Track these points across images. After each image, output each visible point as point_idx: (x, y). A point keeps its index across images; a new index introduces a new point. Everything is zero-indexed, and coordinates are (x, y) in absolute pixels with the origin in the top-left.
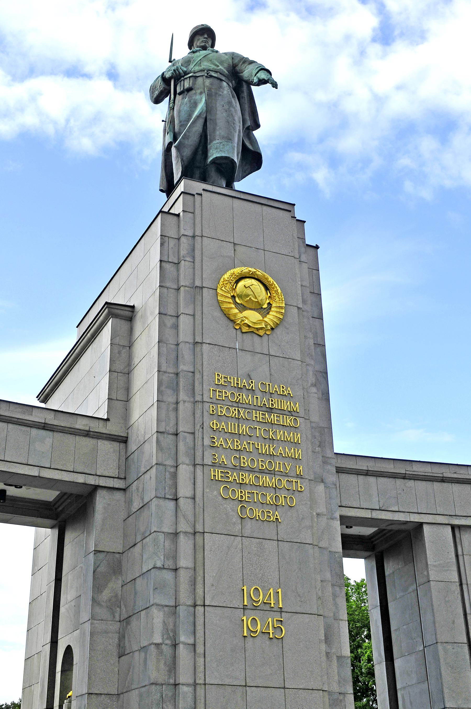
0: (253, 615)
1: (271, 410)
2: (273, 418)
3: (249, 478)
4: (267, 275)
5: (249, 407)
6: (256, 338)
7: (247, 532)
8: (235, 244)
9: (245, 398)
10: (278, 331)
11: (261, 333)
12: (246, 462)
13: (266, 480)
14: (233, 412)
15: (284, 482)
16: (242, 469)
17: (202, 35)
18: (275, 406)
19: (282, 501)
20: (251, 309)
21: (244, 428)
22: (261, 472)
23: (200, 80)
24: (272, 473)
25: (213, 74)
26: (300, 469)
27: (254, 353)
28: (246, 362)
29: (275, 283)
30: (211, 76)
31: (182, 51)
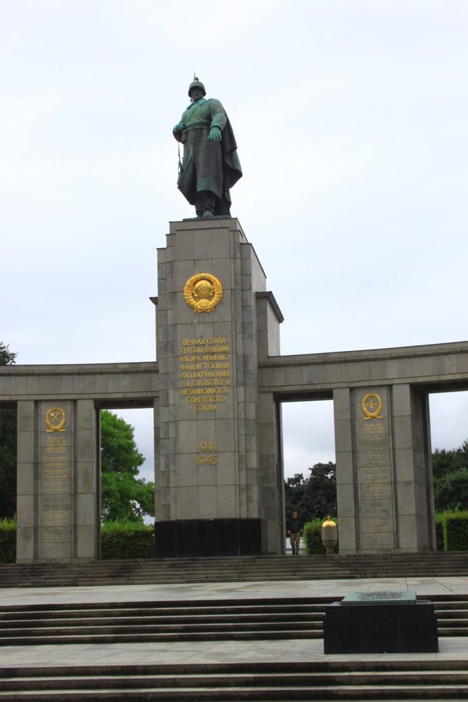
0: (200, 455)
1: (213, 354)
2: (215, 357)
3: (199, 391)
4: (211, 276)
5: (201, 354)
6: (206, 314)
7: (200, 418)
8: (195, 260)
9: (199, 350)
10: (219, 307)
11: (208, 311)
12: (199, 383)
13: (210, 390)
14: (193, 358)
15: (219, 390)
16: (197, 387)
17: (194, 91)
18: (215, 351)
19: (218, 399)
20: (203, 298)
21: (199, 366)
22: (207, 387)
23: (190, 133)
24: (214, 386)
25: (197, 127)
26: (228, 382)
27: (204, 323)
28: (201, 330)
29: (216, 279)
30: (196, 129)
31: (188, 101)
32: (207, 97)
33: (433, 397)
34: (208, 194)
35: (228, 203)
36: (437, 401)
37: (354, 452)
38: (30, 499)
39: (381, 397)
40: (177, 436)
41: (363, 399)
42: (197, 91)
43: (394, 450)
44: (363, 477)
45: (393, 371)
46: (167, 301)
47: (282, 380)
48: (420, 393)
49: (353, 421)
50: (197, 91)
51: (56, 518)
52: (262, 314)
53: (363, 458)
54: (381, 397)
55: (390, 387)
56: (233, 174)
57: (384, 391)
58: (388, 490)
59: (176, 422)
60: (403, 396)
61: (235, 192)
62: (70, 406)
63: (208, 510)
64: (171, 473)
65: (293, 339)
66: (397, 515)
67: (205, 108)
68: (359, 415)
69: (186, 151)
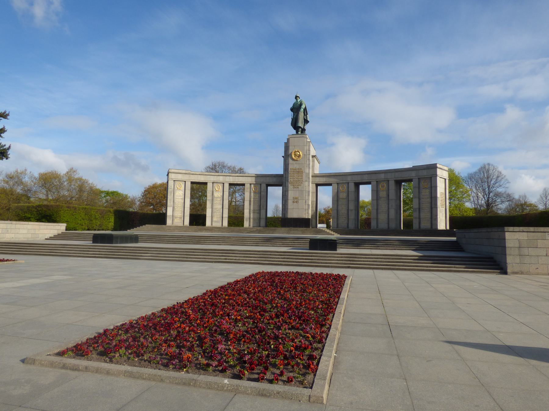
33: (361, 187)
34: (300, 127)
36: (361, 187)
37: (338, 201)
38: (248, 210)
39: (345, 186)
44: (340, 208)
45: (349, 178)
46: (287, 156)
48: (357, 186)
49: (338, 192)
50: (296, 97)
52: (313, 161)
53: (340, 203)
58: (346, 212)
59: (288, 191)
60: (352, 186)
61: (307, 127)
67: (299, 103)
68: (339, 191)
69: (294, 115)
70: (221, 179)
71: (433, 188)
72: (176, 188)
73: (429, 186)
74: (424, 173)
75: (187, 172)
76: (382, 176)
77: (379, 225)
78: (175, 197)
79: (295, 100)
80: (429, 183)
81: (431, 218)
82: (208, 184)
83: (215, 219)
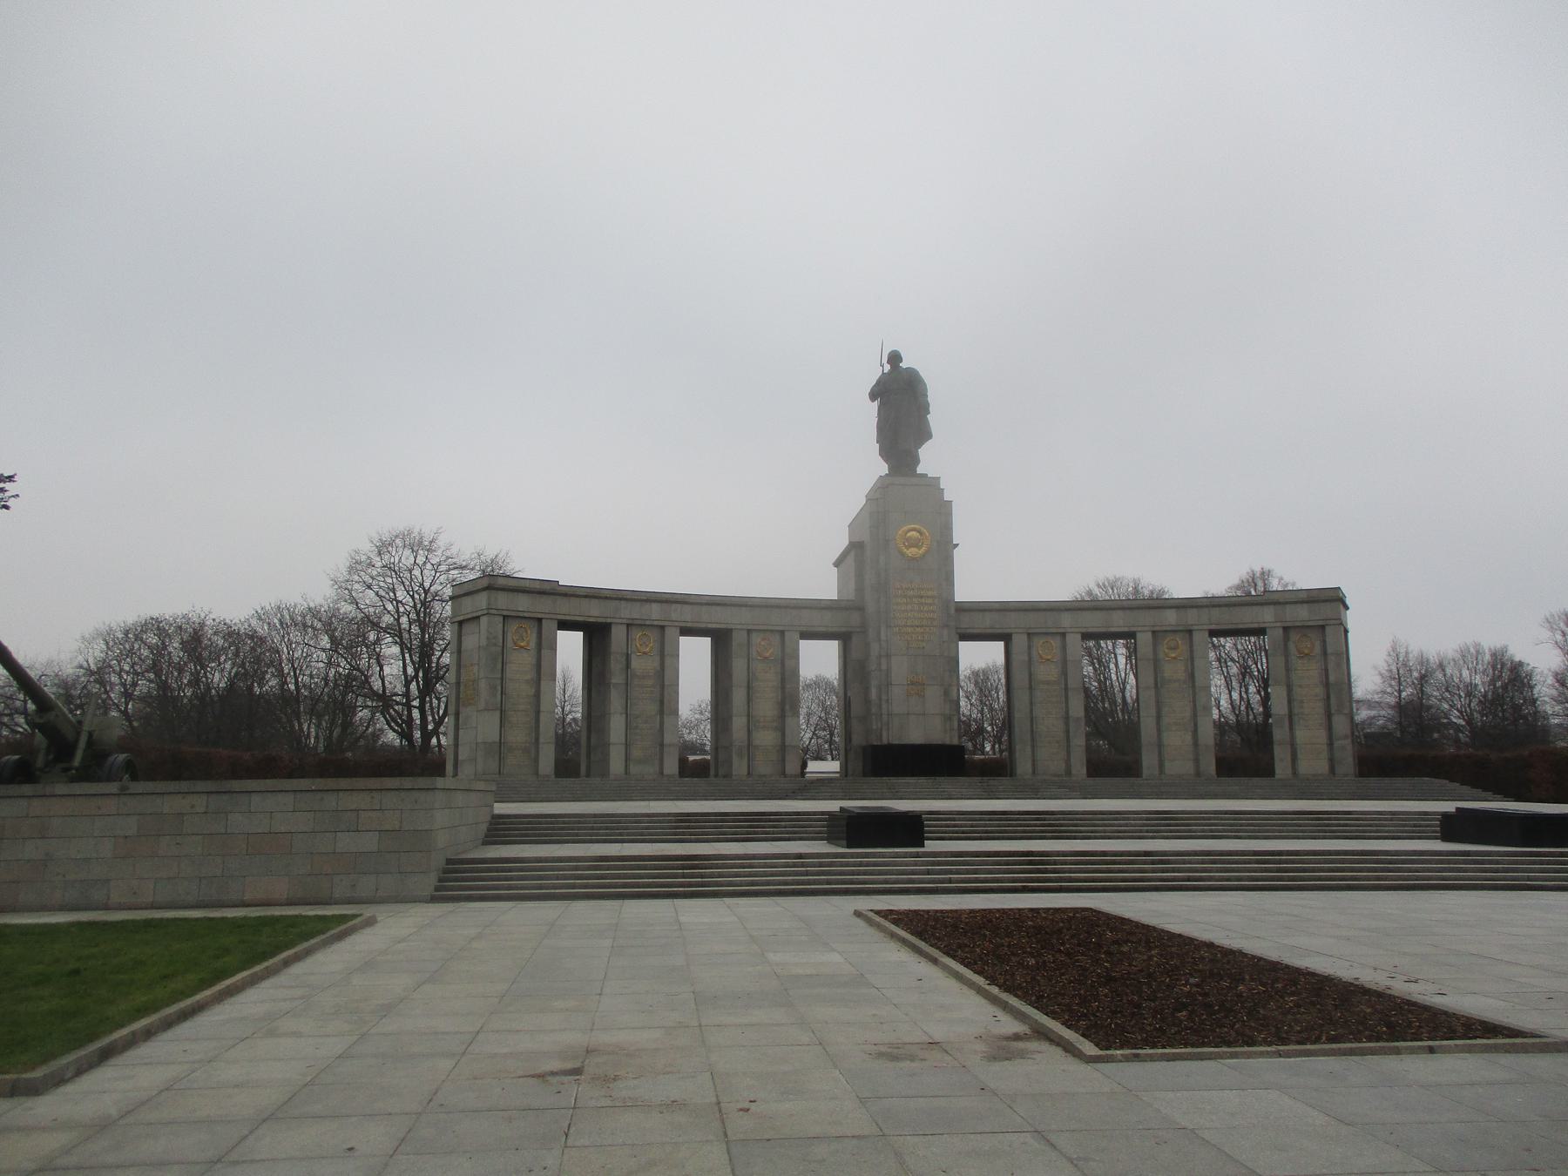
32: (903, 365)
35: (917, 461)
38: (744, 720)
40: (888, 671)
41: (1038, 642)
42: (895, 358)
43: (1066, 689)
45: (1066, 621)
47: (967, 622)
51: (766, 738)
54: (1055, 643)
55: (1063, 635)
56: (924, 434)
57: (1058, 638)
59: (888, 656)
62: (778, 637)
63: (916, 735)
64: (884, 706)
65: (968, 588)
66: (1068, 746)
70: (655, 613)
71: (1332, 658)
72: (509, 644)
73: (1318, 649)
74: (1302, 614)
75: (547, 587)
76: (1171, 618)
77: (1167, 764)
78: (509, 674)
79: (887, 368)
80: (1318, 645)
81: (1331, 744)
82: (614, 629)
83: (636, 753)
